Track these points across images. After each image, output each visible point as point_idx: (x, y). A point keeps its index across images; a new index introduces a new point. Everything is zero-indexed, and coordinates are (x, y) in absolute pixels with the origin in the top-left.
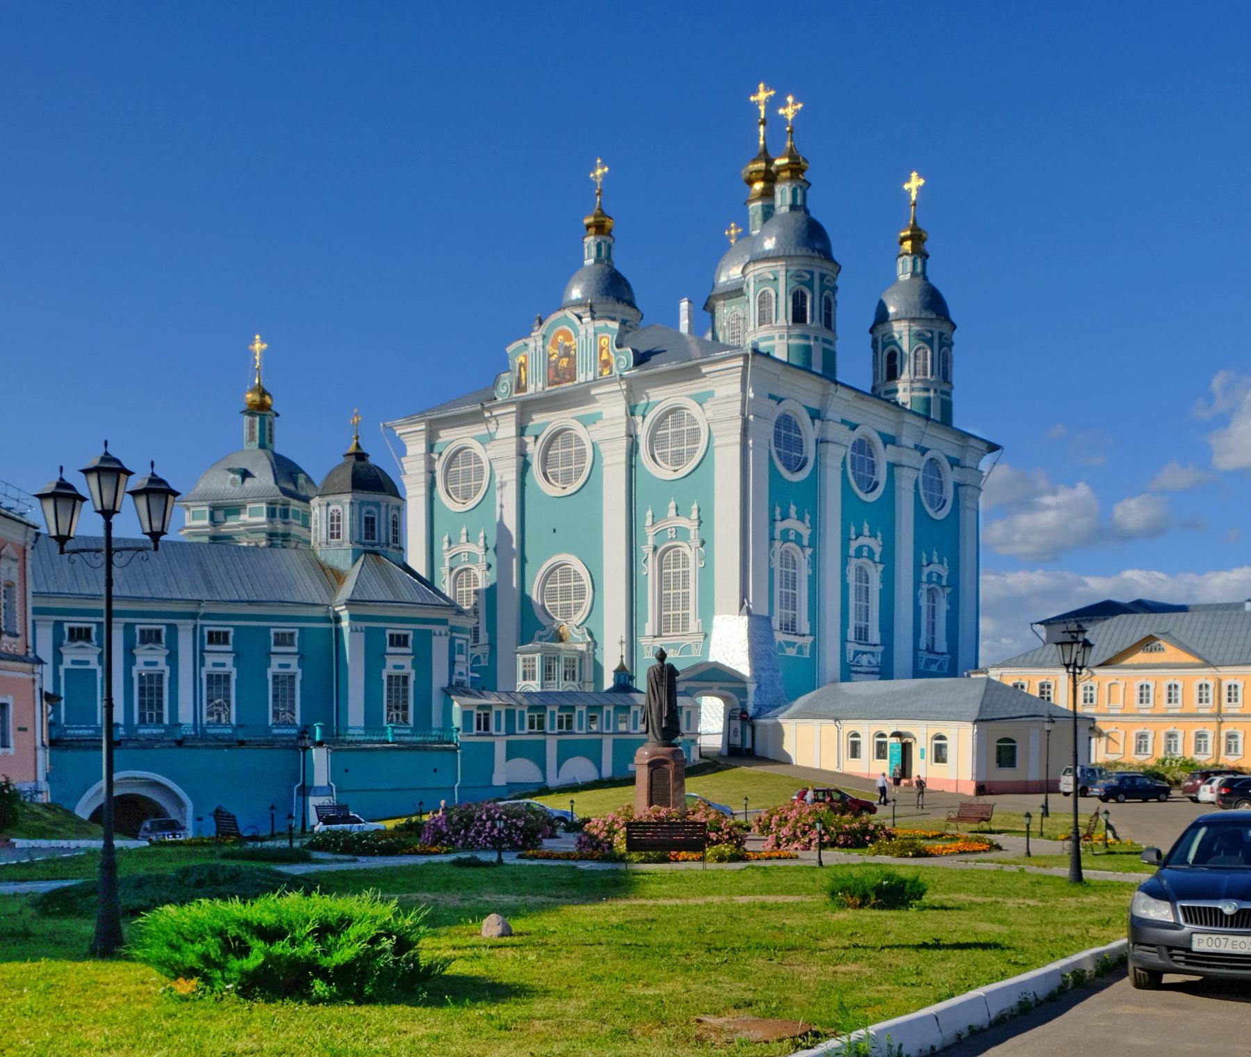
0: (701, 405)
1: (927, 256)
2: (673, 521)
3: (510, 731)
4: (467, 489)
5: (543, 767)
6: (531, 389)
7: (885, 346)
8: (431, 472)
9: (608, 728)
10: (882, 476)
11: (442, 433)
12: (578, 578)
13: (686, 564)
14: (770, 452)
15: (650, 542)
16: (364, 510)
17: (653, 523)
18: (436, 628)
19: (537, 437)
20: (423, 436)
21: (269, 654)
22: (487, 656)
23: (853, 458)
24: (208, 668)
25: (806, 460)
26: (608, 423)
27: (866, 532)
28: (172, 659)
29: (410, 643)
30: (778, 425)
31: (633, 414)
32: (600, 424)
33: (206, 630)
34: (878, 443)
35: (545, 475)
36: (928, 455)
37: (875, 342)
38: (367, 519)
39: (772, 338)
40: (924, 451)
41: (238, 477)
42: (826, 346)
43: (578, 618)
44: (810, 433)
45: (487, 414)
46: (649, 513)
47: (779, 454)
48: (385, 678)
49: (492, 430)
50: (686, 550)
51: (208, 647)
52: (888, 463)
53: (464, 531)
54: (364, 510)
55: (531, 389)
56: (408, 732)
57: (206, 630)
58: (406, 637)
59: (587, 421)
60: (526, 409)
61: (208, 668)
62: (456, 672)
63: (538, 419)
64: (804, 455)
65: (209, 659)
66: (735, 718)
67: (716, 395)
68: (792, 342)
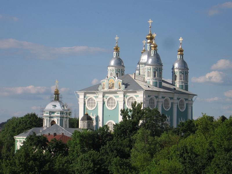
8: (85, 102)
10: (170, 105)
11: (87, 95)
19: (106, 98)
20: (83, 95)
31: (124, 97)
32: (119, 98)
34: (169, 99)
35: (108, 105)
36: (180, 100)
39: (150, 80)
41: (54, 107)
44: (156, 101)
45: (97, 93)
47: (150, 105)
49: (98, 96)
52: (171, 103)
53: (91, 114)
60: (104, 93)
63: (106, 95)
67: (139, 96)
68: (154, 81)
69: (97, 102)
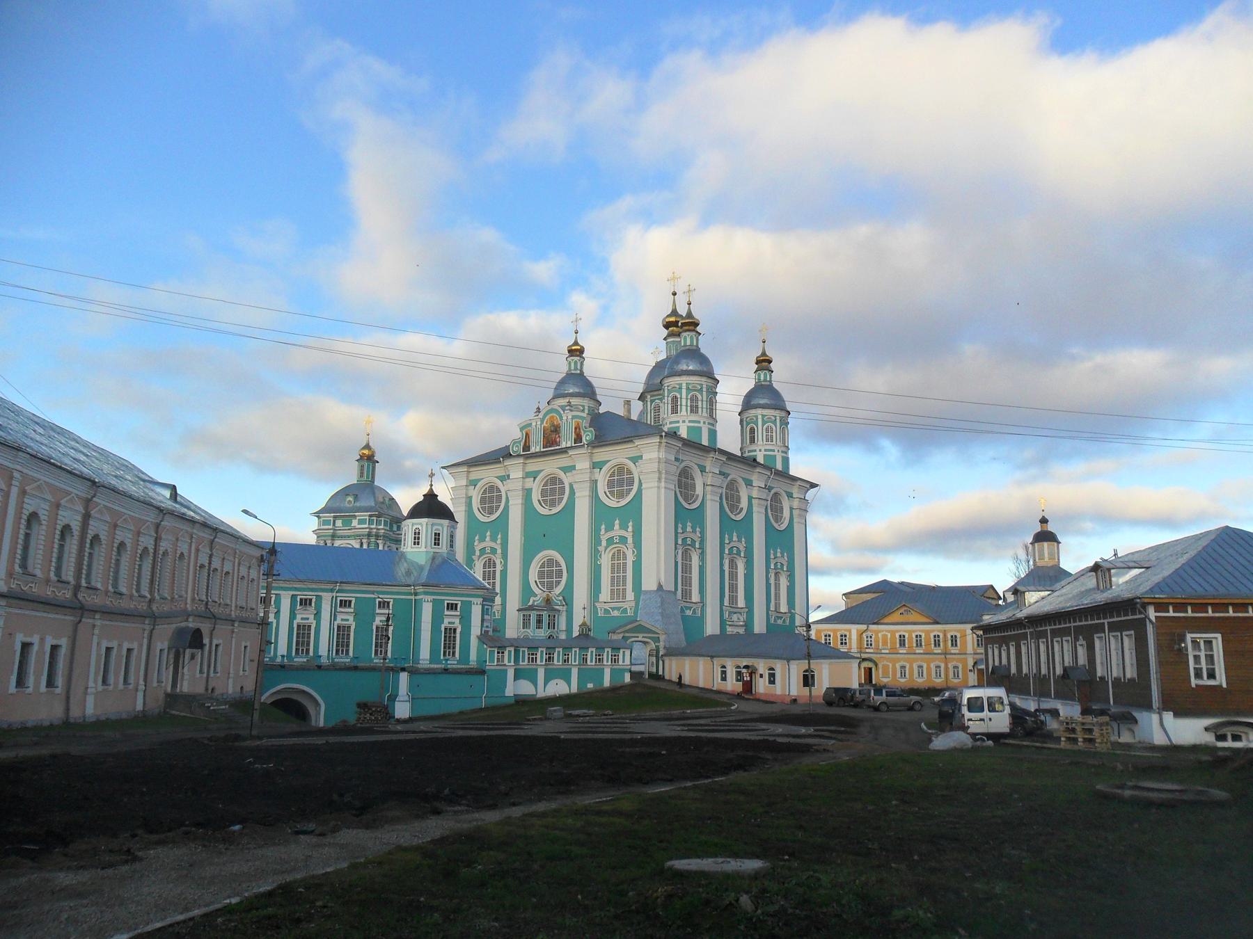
0: (635, 464)
1: (772, 372)
2: (617, 531)
3: (516, 660)
4: (491, 508)
5: (535, 684)
6: (533, 450)
7: (748, 424)
9: (575, 662)
12: (558, 565)
13: (625, 558)
14: (675, 492)
15: (604, 543)
16: (434, 528)
17: (606, 532)
18: (474, 600)
19: (535, 478)
21: (374, 615)
22: (500, 612)
23: (726, 493)
24: (338, 621)
25: (698, 496)
26: (579, 472)
27: (735, 538)
28: (318, 615)
29: (459, 609)
30: (680, 475)
32: (574, 472)
33: (339, 599)
37: (741, 421)
38: (435, 534)
39: (678, 422)
40: (770, 489)
42: (712, 427)
43: (558, 590)
46: (603, 527)
47: (681, 492)
48: (443, 629)
50: (626, 550)
51: (339, 609)
54: (435, 528)
55: (533, 450)
56: (456, 662)
57: (339, 599)
58: (456, 605)
59: (568, 469)
61: (338, 621)
62: (485, 626)
64: (697, 493)
65: (339, 617)
66: (652, 655)
69: (507, 494)
